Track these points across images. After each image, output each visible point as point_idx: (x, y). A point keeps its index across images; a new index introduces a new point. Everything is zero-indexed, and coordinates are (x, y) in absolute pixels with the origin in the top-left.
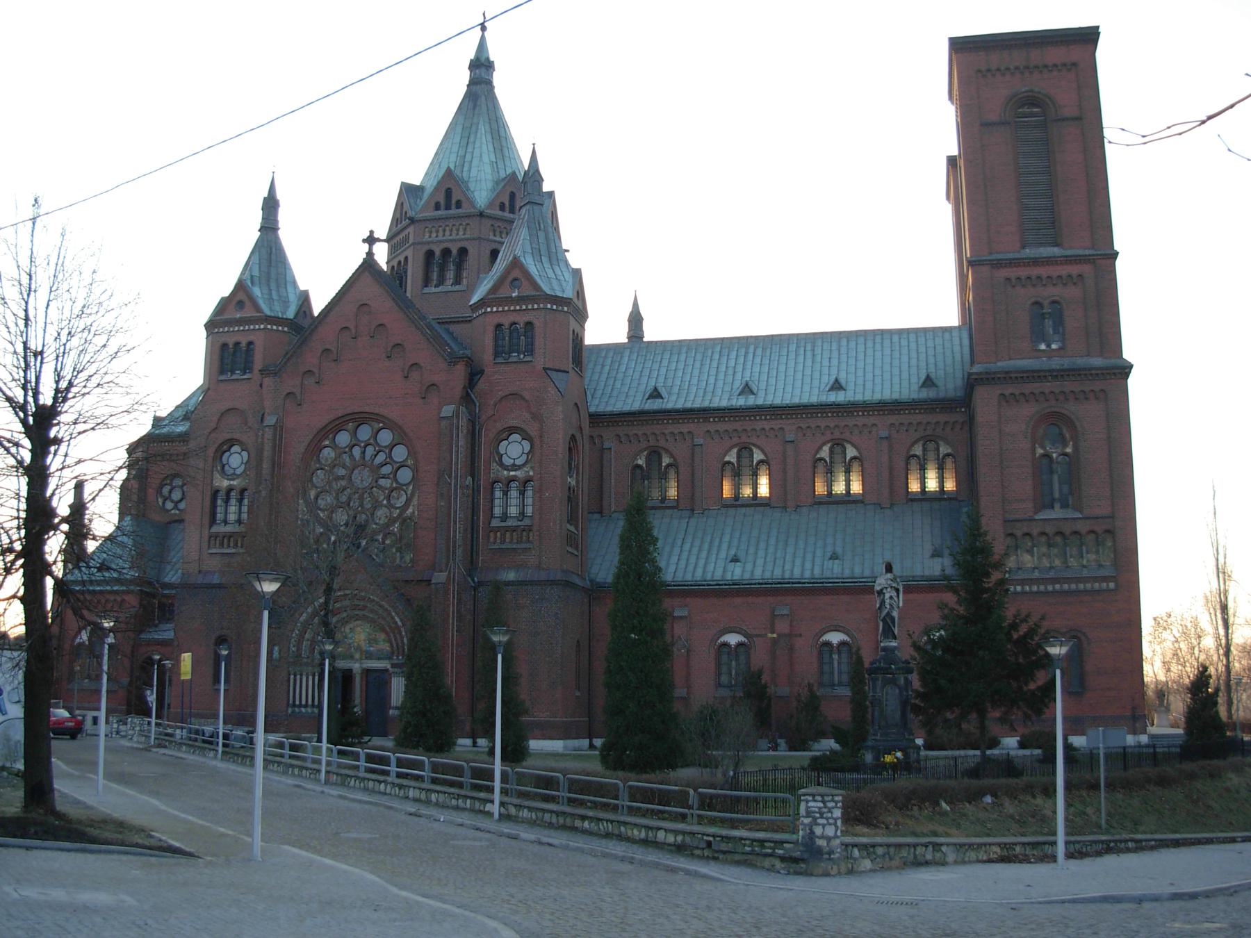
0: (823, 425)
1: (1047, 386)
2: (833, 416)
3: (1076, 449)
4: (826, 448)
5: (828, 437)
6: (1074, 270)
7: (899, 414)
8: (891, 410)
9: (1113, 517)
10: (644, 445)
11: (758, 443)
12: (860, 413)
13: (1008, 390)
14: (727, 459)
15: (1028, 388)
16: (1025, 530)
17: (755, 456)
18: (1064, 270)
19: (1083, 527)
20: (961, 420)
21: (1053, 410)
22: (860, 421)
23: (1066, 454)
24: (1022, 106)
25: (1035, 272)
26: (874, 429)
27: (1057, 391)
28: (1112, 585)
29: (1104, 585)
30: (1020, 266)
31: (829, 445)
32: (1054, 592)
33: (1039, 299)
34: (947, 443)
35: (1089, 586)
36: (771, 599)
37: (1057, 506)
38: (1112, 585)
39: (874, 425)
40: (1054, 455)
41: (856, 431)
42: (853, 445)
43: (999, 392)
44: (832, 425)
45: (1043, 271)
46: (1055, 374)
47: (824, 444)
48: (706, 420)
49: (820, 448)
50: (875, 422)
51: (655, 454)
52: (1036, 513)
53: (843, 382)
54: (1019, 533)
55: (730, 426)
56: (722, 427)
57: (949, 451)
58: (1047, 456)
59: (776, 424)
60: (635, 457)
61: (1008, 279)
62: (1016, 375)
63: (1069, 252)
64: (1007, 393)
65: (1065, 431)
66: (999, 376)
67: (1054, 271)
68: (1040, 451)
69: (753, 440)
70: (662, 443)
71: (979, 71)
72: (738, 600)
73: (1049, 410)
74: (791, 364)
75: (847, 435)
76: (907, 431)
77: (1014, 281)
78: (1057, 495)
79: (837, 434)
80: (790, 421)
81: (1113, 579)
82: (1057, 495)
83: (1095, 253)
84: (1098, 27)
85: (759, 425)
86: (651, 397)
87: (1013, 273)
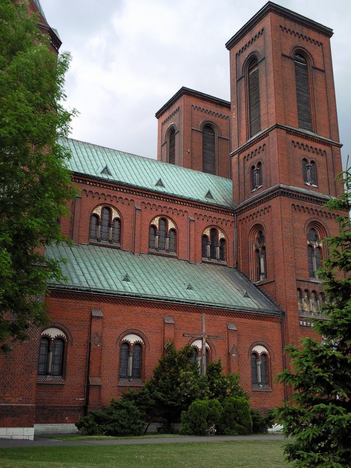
2: (163, 200)
4: (157, 219)
5: (159, 212)
6: (323, 148)
7: (200, 208)
8: (196, 205)
11: (116, 206)
12: (179, 203)
13: (297, 202)
14: (95, 212)
16: (306, 287)
17: (113, 214)
18: (319, 146)
20: (231, 221)
21: (316, 220)
22: (179, 207)
25: (306, 142)
26: (186, 214)
31: (159, 218)
33: (307, 158)
34: (223, 232)
36: (161, 311)
39: (186, 211)
40: (315, 246)
41: (176, 213)
44: (162, 206)
45: (310, 143)
46: (319, 200)
47: (156, 216)
48: (84, 182)
49: (154, 219)
50: (187, 210)
53: (164, 183)
55: (100, 191)
56: (95, 189)
57: (223, 237)
59: (130, 197)
61: (293, 142)
62: (301, 195)
64: (296, 204)
65: (318, 233)
66: (293, 193)
68: (308, 243)
69: (114, 203)
71: (281, 27)
72: (139, 309)
73: (313, 220)
75: (170, 214)
76: (203, 219)
77: (296, 143)
79: (164, 213)
80: (138, 197)
83: (332, 141)
84: (332, 30)
85: (119, 194)
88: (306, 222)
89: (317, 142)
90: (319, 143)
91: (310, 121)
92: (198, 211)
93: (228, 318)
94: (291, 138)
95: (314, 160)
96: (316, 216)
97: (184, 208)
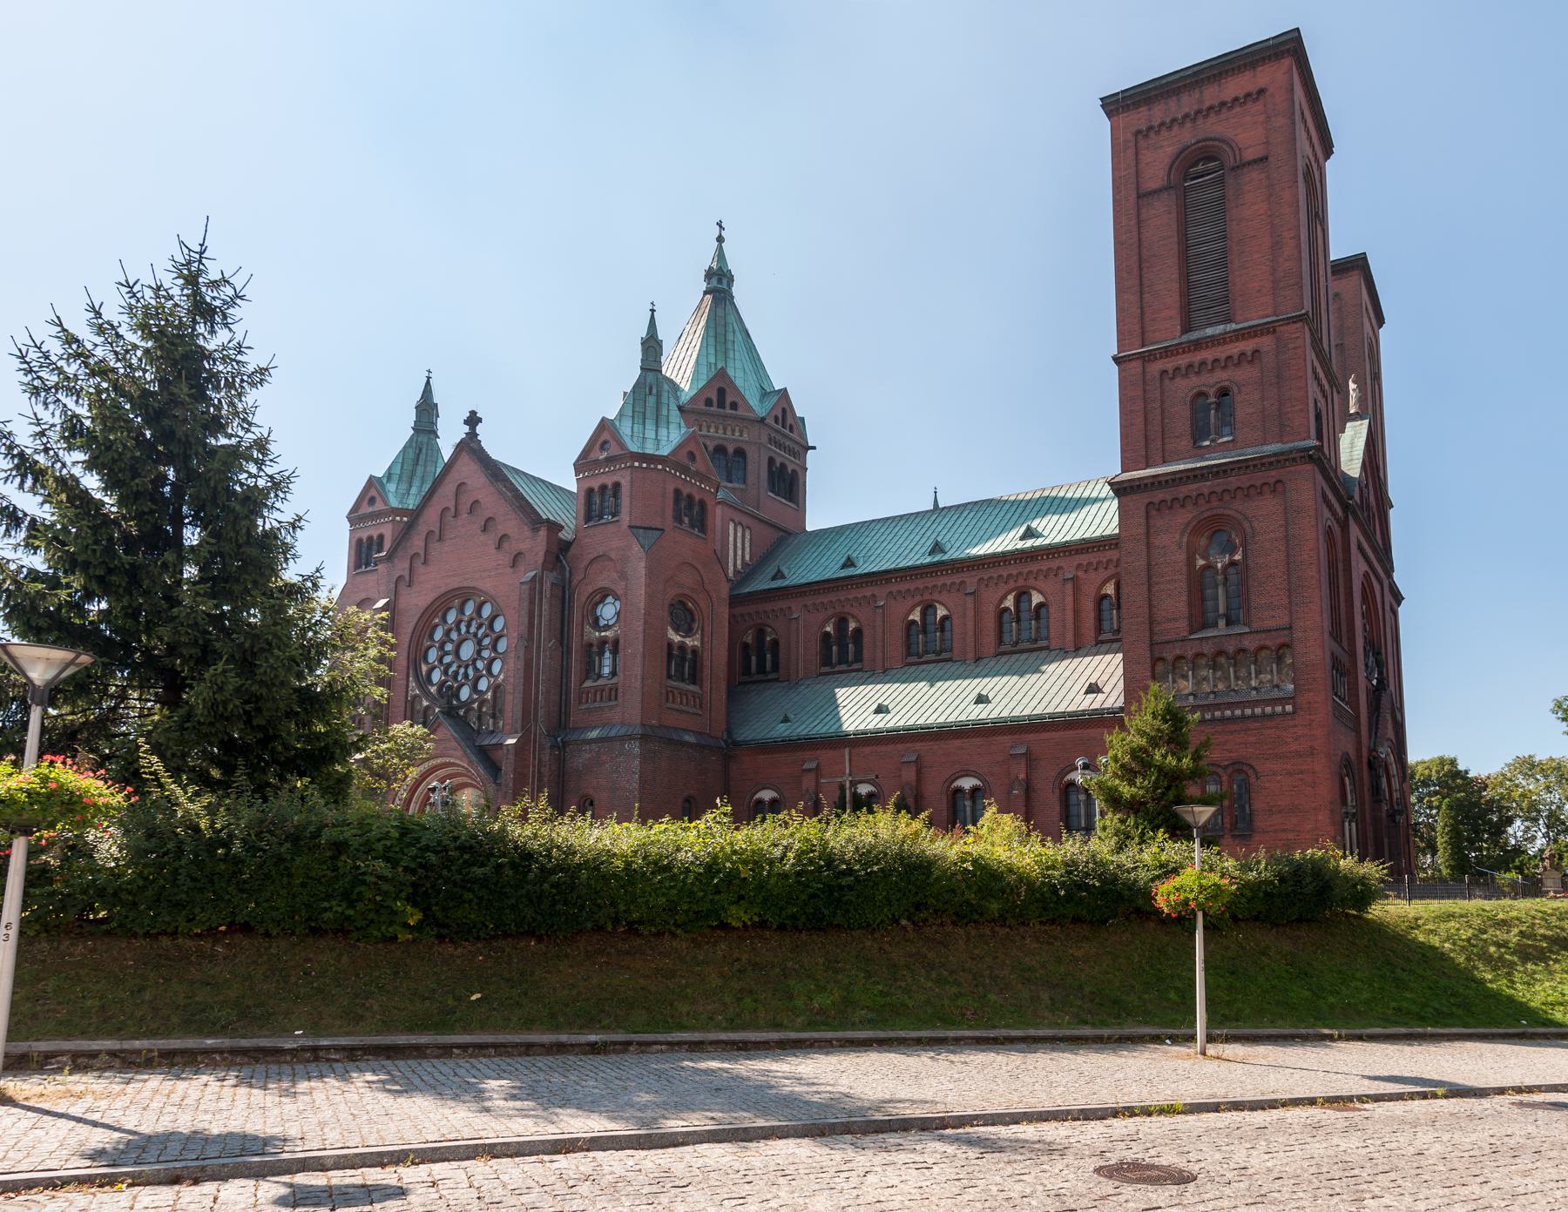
0: (1005, 574)
1: (1206, 486)
3: (1245, 555)
4: (1011, 598)
6: (1247, 346)
9: (1290, 628)
10: (830, 612)
13: (1158, 496)
14: (911, 617)
15: (1184, 490)
18: (1235, 349)
19: (1250, 643)
21: (1215, 512)
23: (1233, 564)
24: (1195, 164)
25: (1197, 357)
27: (1218, 489)
28: (1289, 708)
29: (1279, 709)
30: (1178, 353)
32: (1213, 720)
33: (1204, 389)
35: (1258, 711)
37: (1222, 623)
38: (1289, 708)
39: (1059, 568)
40: (1219, 565)
42: (1040, 592)
43: (1146, 501)
44: (1014, 573)
45: (1207, 355)
47: (1009, 593)
48: (888, 581)
49: (1004, 597)
51: (842, 622)
52: (1191, 633)
54: (1169, 657)
55: (911, 586)
56: (903, 587)
58: (1209, 567)
59: (957, 578)
60: (824, 626)
63: (1241, 326)
67: (1221, 352)
68: (1201, 562)
70: (847, 609)
74: (997, 520)
75: (1031, 582)
78: (1222, 610)
79: (1021, 582)
81: (1290, 699)
82: (1222, 610)
85: (940, 581)
86: (844, 566)
87: (1169, 364)
88: (1186, 528)
89: (1231, 341)
90: (1237, 340)
91: (1226, 300)
92: (1084, 559)
93: (1017, 736)
94: (1156, 367)
95: (1227, 383)
96: (1215, 504)
97: (1055, 564)
